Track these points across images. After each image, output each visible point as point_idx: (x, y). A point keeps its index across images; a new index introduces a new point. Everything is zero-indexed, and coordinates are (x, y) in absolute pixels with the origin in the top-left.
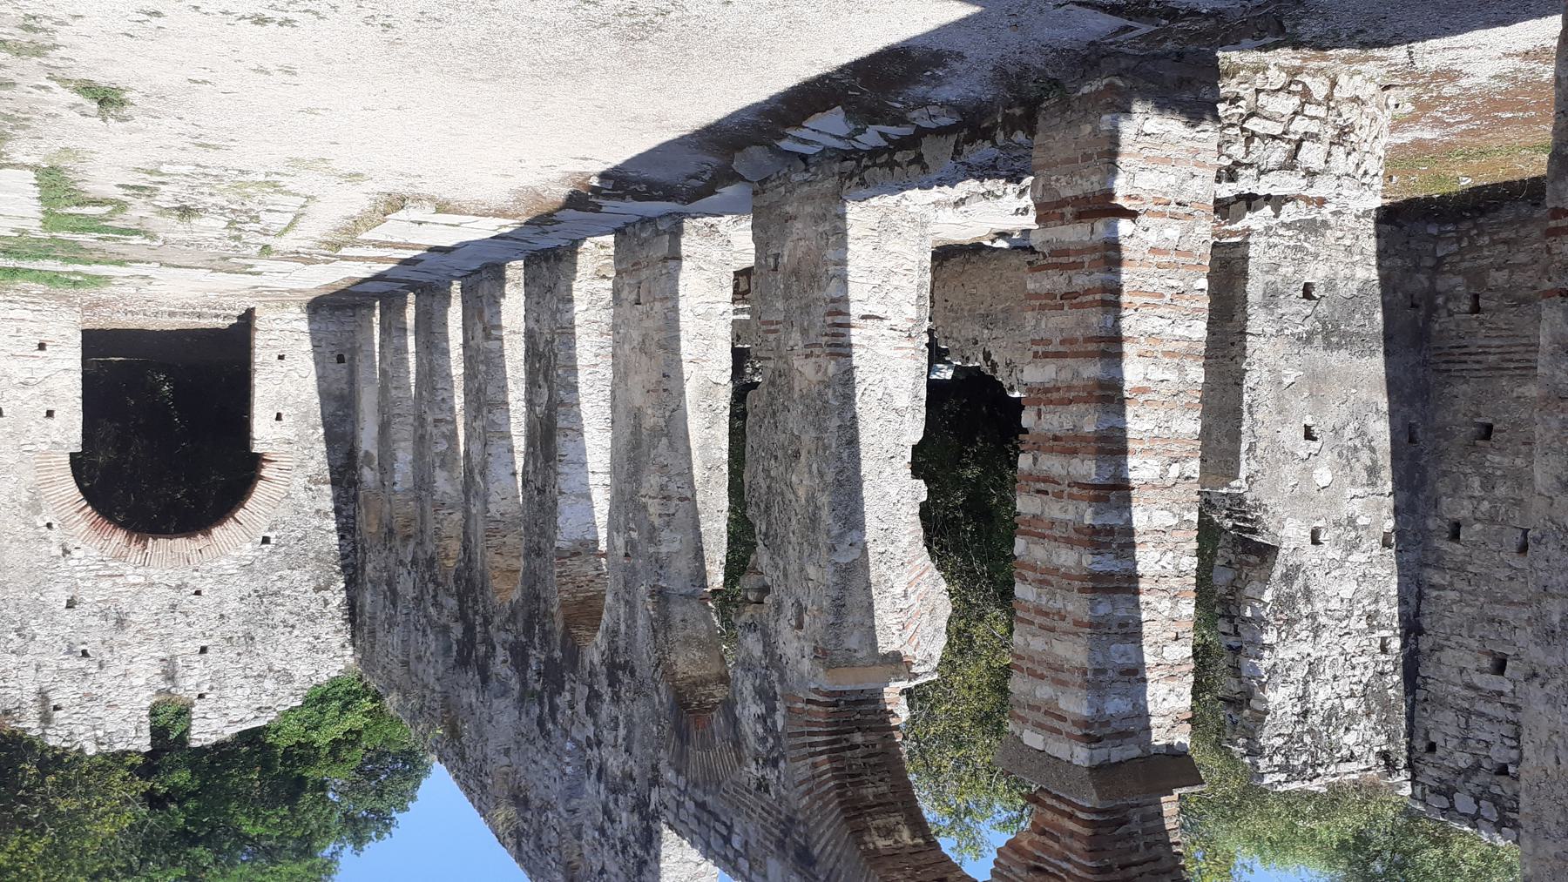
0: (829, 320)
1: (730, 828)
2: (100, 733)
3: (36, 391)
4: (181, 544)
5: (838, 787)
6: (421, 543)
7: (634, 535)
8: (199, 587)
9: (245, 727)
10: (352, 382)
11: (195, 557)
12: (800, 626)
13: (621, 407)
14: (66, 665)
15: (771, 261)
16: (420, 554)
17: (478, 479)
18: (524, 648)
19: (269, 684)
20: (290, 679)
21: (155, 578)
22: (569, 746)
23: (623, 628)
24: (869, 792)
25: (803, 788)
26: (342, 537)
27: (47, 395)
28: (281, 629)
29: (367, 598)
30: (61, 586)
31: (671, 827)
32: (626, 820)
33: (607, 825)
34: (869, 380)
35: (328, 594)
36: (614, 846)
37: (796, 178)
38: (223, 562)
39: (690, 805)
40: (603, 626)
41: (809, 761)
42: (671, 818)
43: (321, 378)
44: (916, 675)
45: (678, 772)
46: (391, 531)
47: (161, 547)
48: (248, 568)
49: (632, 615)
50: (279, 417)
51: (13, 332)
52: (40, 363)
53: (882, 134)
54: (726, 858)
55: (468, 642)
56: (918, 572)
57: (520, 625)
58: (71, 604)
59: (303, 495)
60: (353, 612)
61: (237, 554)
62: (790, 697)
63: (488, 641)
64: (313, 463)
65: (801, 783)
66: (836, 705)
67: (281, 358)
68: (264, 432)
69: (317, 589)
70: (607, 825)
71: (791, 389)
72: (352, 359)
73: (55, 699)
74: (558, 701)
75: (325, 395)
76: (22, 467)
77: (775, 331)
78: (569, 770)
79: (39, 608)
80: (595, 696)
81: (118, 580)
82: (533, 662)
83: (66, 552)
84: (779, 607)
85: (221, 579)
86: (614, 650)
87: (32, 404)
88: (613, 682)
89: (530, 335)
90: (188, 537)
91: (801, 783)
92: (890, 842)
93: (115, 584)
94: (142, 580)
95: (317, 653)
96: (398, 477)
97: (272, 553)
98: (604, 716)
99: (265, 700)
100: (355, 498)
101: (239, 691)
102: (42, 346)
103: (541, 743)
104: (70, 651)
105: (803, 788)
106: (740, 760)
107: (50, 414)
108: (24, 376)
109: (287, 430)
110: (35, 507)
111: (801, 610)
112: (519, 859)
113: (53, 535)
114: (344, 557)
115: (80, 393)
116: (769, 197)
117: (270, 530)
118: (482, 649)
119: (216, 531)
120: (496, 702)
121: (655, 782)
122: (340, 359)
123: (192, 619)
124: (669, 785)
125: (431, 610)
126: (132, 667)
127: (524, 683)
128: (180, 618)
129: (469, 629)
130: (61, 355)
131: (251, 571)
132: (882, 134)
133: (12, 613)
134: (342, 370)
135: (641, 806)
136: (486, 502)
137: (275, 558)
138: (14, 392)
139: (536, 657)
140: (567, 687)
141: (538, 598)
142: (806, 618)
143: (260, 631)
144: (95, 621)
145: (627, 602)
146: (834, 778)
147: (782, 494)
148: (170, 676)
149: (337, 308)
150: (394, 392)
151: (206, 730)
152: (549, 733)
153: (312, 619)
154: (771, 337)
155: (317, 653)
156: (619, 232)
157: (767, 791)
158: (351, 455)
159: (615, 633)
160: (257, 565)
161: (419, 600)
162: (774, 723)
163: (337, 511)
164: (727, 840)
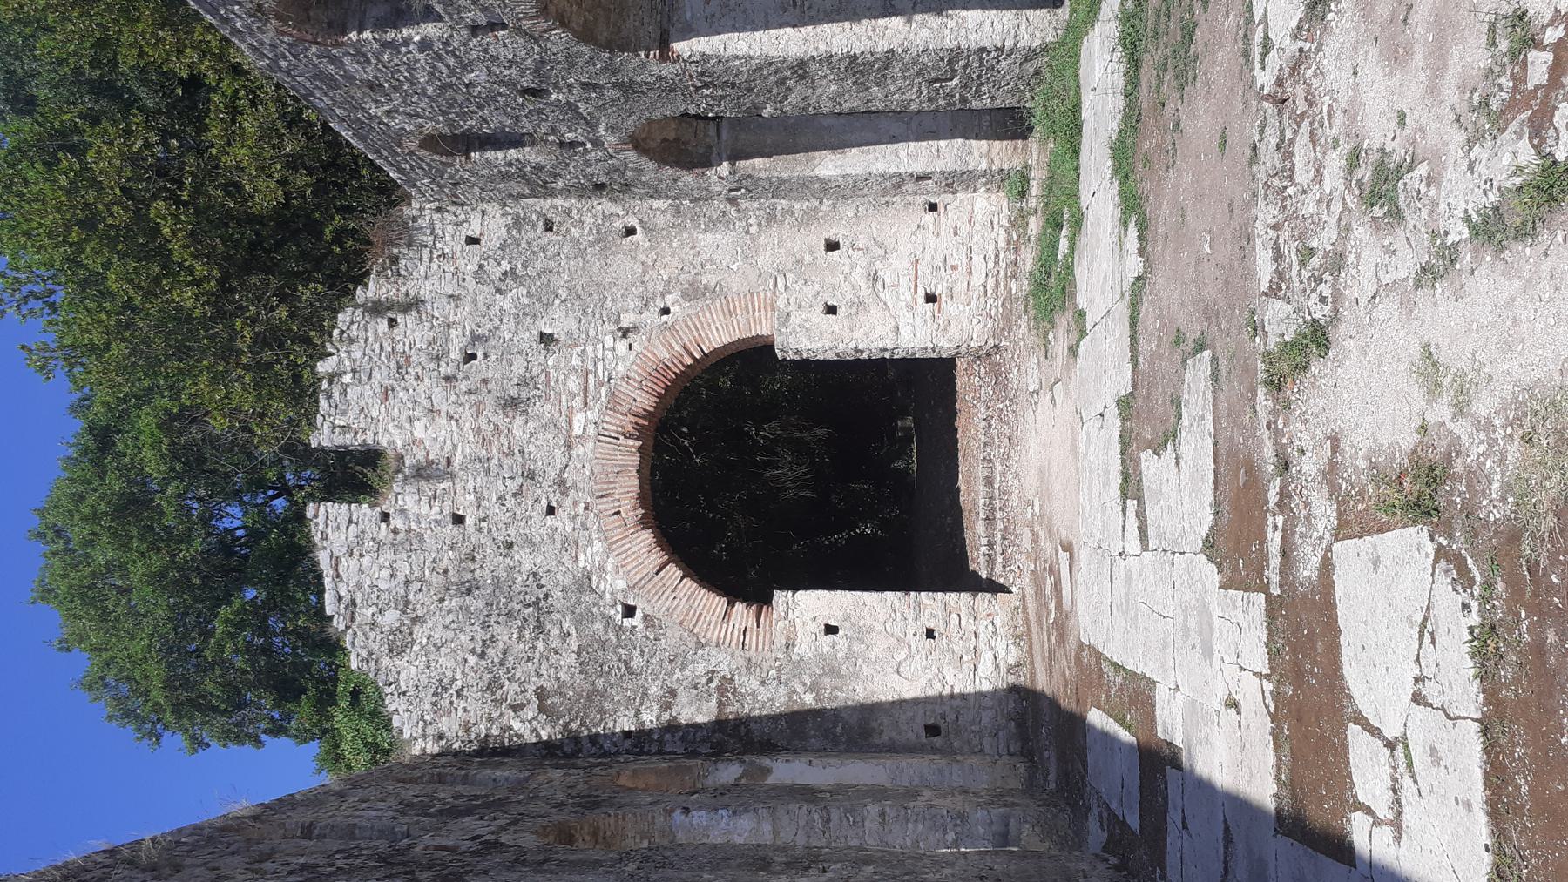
2: (347, 379)
3: (865, 291)
4: (630, 485)
8: (560, 512)
9: (327, 581)
10: (892, 749)
11: (608, 506)
14: (454, 333)
19: (391, 618)
20: (396, 650)
21: (579, 450)
26: (627, 734)
27: (859, 305)
28: (481, 635)
29: (508, 772)
30: (574, 326)
35: (530, 712)
38: (598, 546)
43: (901, 704)
46: (596, 805)
47: (628, 456)
48: (584, 584)
50: (831, 630)
51: (950, 261)
52: (906, 295)
58: (546, 339)
59: (701, 668)
60: (491, 752)
61: (609, 567)
64: (754, 684)
67: (930, 634)
68: (804, 609)
69: (541, 694)
72: (934, 750)
73: (407, 321)
75: (869, 711)
76: (753, 276)
79: (544, 299)
83: (625, 332)
85: (570, 544)
87: (846, 287)
90: (642, 497)
93: (573, 396)
94: (577, 430)
95: (433, 686)
96: (699, 818)
97: (608, 621)
99: (365, 613)
100: (694, 754)
101: (386, 573)
102: (931, 298)
104: (475, 338)
107: (831, 310)
108: (887, 276)
109: (809, 643)
110: (693, 292)
113: (651, 317)
114: (594, 739)
117: (646, 617)
119: (647, 536)
122: (932, 730)
123: (510, 502)
126: (443, 421)
128: (512, 486)
130: (918, 322)
131: (580, 589)
133: (538, 265)
134: (915, 734)
137: (598, 626)
138: (864, 264)
143: (481, 604)
144: (519, 367)
148: (423, 472)
149: (1021, 725)
150: (873, 810)
151: (334, 526)
153: (493, 685)
155: (433, 686)
160: (590, 598)
163: (672, 727)
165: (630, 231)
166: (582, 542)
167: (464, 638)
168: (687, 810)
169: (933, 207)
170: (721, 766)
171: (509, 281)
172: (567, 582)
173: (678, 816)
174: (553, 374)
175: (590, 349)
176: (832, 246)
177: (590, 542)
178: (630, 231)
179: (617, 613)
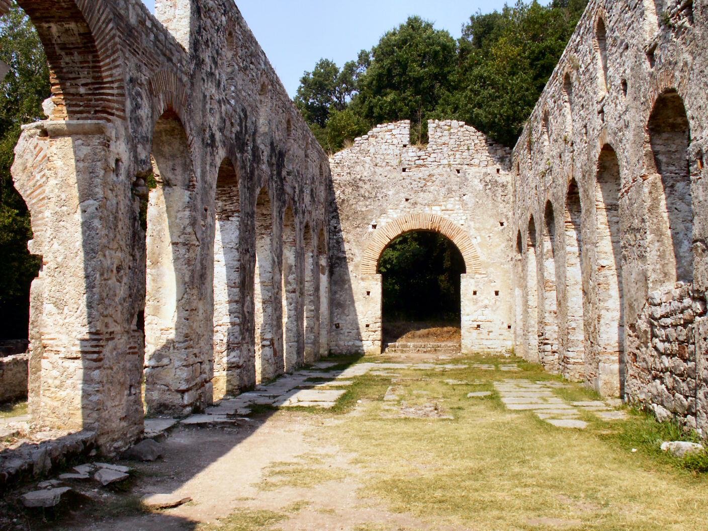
0: (102, 356)
1: (155, 45)
3: (480, 304)
5: (99, 62)
6: (301, 223)
7: (203, 223)
8: (407, 203)
10: (331, 313)
12: (117, 161)
13: (209, 299)
15: (133, 391)
16: (301, 216)
17: (276, 259)
18: (254, 160)
22: (233, 102)
23: (208, 168)
24: (77, 57)
25: (117, 63)
27: (476, 302)
28: (366, 179)
29: (322, 194)
31: (184, 49)
32: (206, 56)
33: (216, 56)
34: (74, 318)
36: (213, 43)
37: (120, 443)
38: (395, 216)
39: (174, 59)
40: (217, 170)
41: (114, 79)
42: (184, 55)
44: (37, 127)
45: (181, 80)
47: (425, 225)
48: (383, 212)
49: (204, 173)
50: (368, 293)
53: (78, 473)
54: (158, 29)
55: (280, 165)
56: (35, 194)
57: (256, 173)
62: (124, 118)
63: (271, 165)
65: (118, 66)
66: (96, 112)
70: (216, 56)
71: (122, 313)
72: (331, 327)
74: (238, 128)
77: (130, 348)
78: (233, 88)
80: (221, 130)
81: (443, 208)
82: (250, 152)
84: (128, 176)
86: (212, 154)
87: (482, 298)
88: (212, 136)
89: (253, 343)
91: (118, 66)
92: (67, 26)
93: (446, 206)
94: (434, 208)
96: (311, 260)
97: (371, 220)
98: (218, 116)
103: (245, 105)
105: (117, 63)
106: (150, 83)
107: (475, 293)
108: (486, 311)
111: (116, 171)
112: (256, 43)
115: (462, 304)
116: (134, 429)
117: (371, 233)
118: (274, 160)
120: (267, 130)
121: (192, 77)
122: (337, 326)
123: (410, 187)
124: (186, 74)
125: (297, 186)
127: (254, 141)
129: (279, 174)
132: (78, 473)
135: (200, 63)
136: (272, 244)
137: (370, 217)
138: (491, 304)
139: (249, 156)
140: (234, 136)
141: (248, 188)
142: (114, 166)
143: (377, 178)
145: (206, 182)
146: (100, 67)
147: (127, 245)
151: (401, 129)
152: (243, 110)
154: (132, 345)
156: (211, 405)
157: (137, 64)
158: (331, 273)
159: (211, 165)
160: (378, 214)
161: (301, 191)
162: (132, 104)
164: (156, 37)
165: (502, 224)
166: (397, 211)
167: (365, 174)
168: (312, 257)
169: (509, 327)
170: (326, 260)
171: (484, 184)
172: (384, 207)
173: (311, 254)
174: (452, 199)
175: (461, 211)
176: (497, 293)
177: (397, 213)
178: (502, 224)
179: (373, 223)
